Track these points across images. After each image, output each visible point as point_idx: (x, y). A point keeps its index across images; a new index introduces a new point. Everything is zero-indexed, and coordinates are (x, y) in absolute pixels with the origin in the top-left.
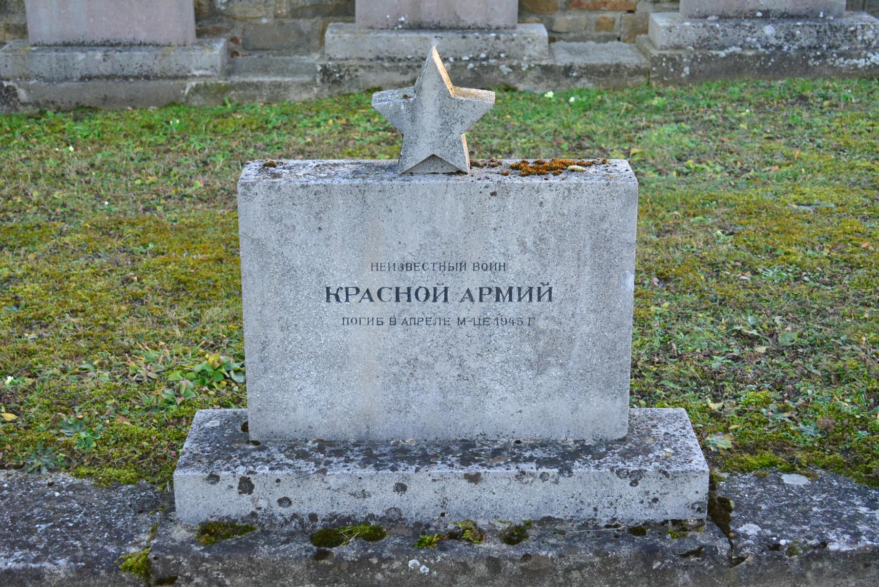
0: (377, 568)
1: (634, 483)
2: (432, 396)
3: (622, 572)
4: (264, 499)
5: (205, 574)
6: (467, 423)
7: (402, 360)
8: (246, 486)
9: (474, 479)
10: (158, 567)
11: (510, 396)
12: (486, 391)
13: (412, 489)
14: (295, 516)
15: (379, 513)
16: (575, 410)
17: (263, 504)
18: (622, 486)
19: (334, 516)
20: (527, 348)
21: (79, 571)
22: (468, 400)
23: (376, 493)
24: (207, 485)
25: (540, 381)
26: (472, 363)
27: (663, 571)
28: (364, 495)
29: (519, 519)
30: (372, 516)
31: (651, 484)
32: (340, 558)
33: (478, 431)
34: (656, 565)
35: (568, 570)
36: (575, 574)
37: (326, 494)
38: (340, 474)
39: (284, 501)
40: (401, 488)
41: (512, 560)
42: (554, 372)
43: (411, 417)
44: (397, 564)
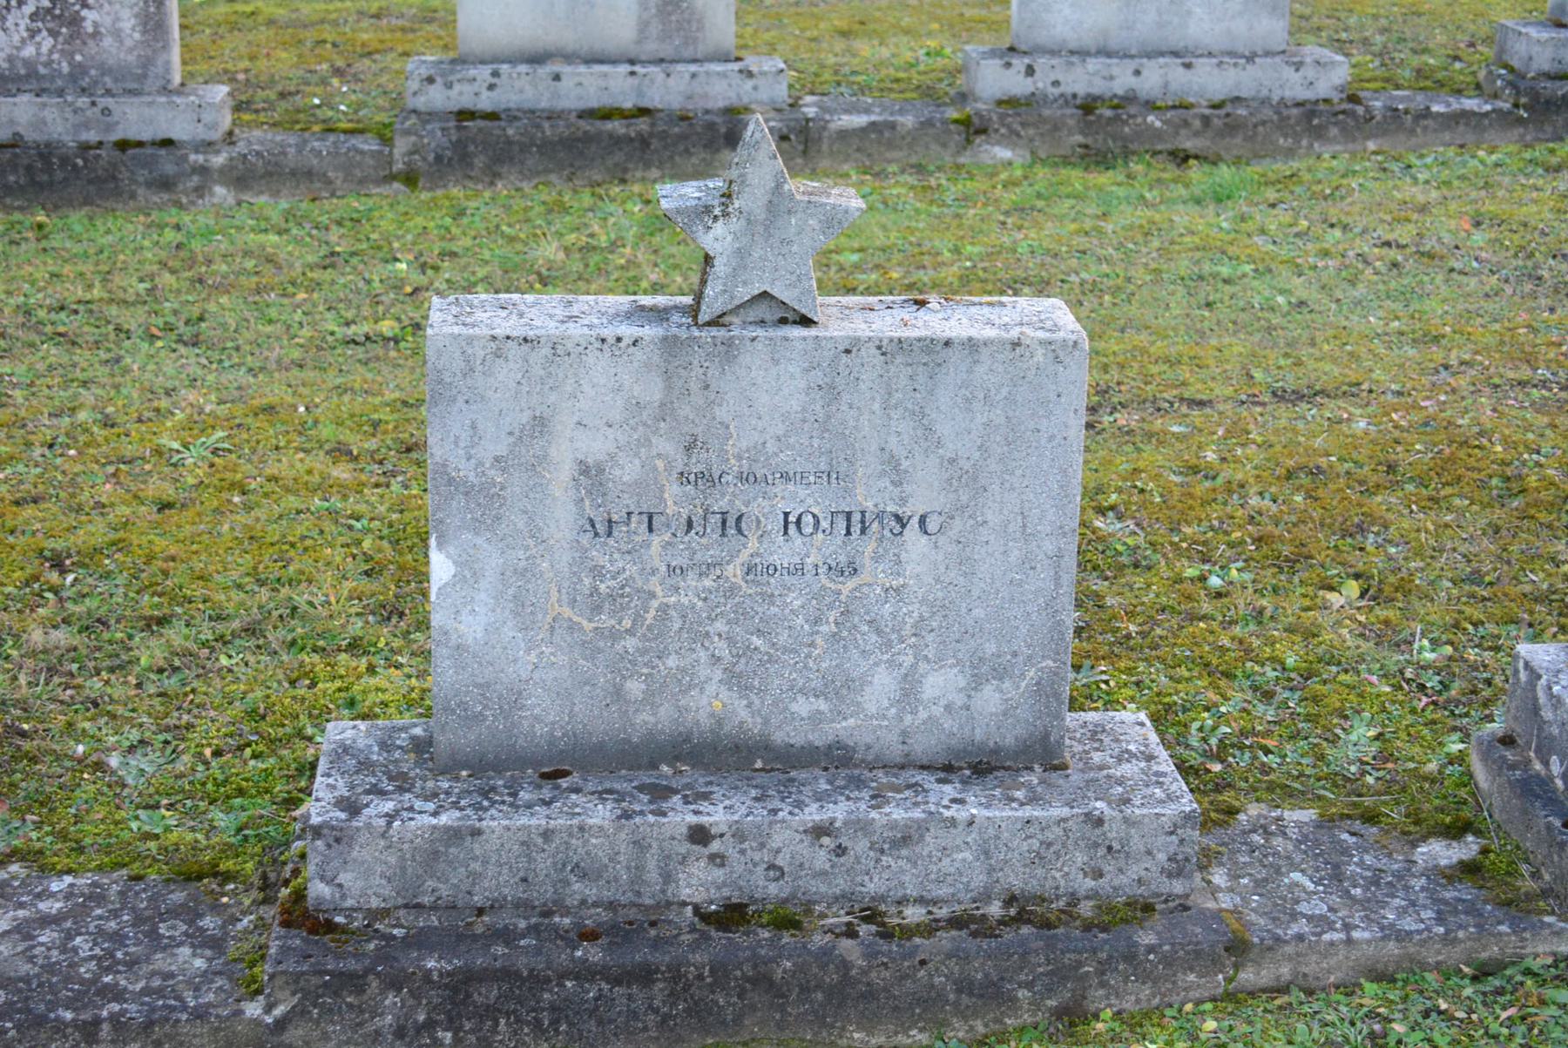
0: (1125, 123)
1: (1297, 70)
3: (1292, 127)
4: (1041, 82)
5: (1009, 127)
8: (1030, 71)
9: (1188, 66)
10: (976, 120)
12: (1189, 13)
13: (1145, 73)
14: (1062, 95)
15: (1120, 92)
16: (1251, 28)
17: (1040, 85)
18: (1289, 73)
19: (1089, 95)
21: (922, 123)
22: (1176, 20)
23: (1122, 80)
24: (1002, 70)
27: (1320, 127)
28: (1112, 78)
29: (1218, 97)
30: (1115, 96)
31: (1309, 72)
32: (1101, 116)
33: (1182, 44)
34: (1316, 122)
35: (1255, 126)
36: (1261, 129)
37: (1081, 80)
38: (1093, 64)
39: (1056, 83)
40: (1137, 73)
41: (1219, 117)
43: (1136, 33)
44: (1139, 120)
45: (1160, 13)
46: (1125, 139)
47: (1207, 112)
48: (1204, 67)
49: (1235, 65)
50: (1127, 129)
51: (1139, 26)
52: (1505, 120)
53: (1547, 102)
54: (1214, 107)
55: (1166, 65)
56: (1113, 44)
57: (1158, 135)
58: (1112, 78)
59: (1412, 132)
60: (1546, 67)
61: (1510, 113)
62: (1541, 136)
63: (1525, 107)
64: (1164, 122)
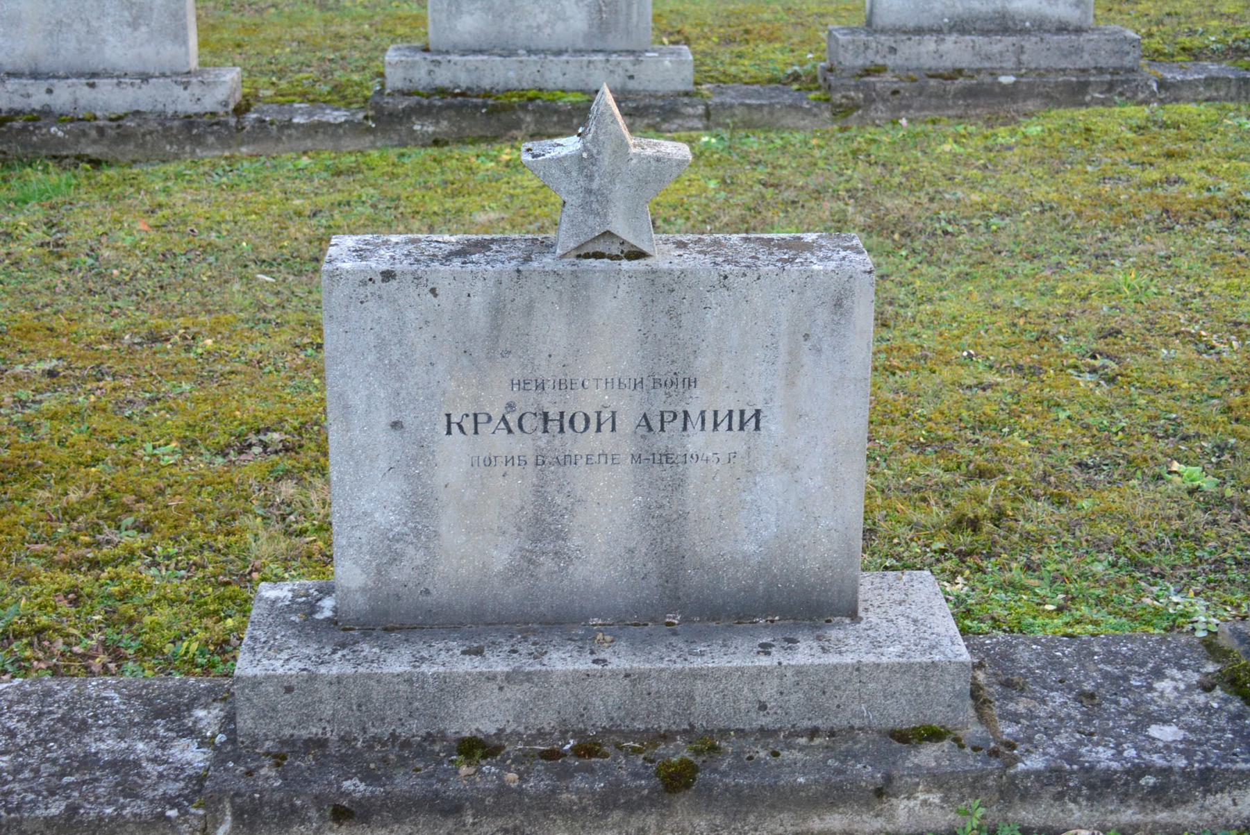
0: (33, 133)
1: (185, 88)
2: (72, 45)
3: (175, 136)
6: (94, 63)
7: (53, 22)
9: (92, 86)
11: (119, 44)
12: (104, 41)
13: (56, 92)
15: (38, 107)
16: (158, 53)
18: (178, 91)
19: (11, 110)
20: (126, 14)
22: (94, 47)
23: (37, 97)
25: (136, 34)
26: (95, 24)
27: (199, 135)
28: (29, 96)
29: (121, 111)
30: (34, 110)
31: (196, 89)
32: (11, 128)
33: (101, 67)
34: (195, 131)
35: (144, 135)
36: (148, 137)
40: (50, 91)
41: (111, 128)
42: (144, 29)
43: (61, 58)
44: (44, 131)
45: (79, 41)
46: (34, 146)
47: (101, 123)
48: (105, 85)
49: (132, 84)
50: (35, 139)
51: (63, 52)
52: (354, 128)
53: (390, 115)
54: (111, 120)
55: (74, 85)
56: (43, 67)
57: (62, 143)
58: (29, 96)
59: (279, 139)
60: (399, 85)
61: (360, 124)
62: (389, 143)
63: (373, 119)
64: (65, 133)
